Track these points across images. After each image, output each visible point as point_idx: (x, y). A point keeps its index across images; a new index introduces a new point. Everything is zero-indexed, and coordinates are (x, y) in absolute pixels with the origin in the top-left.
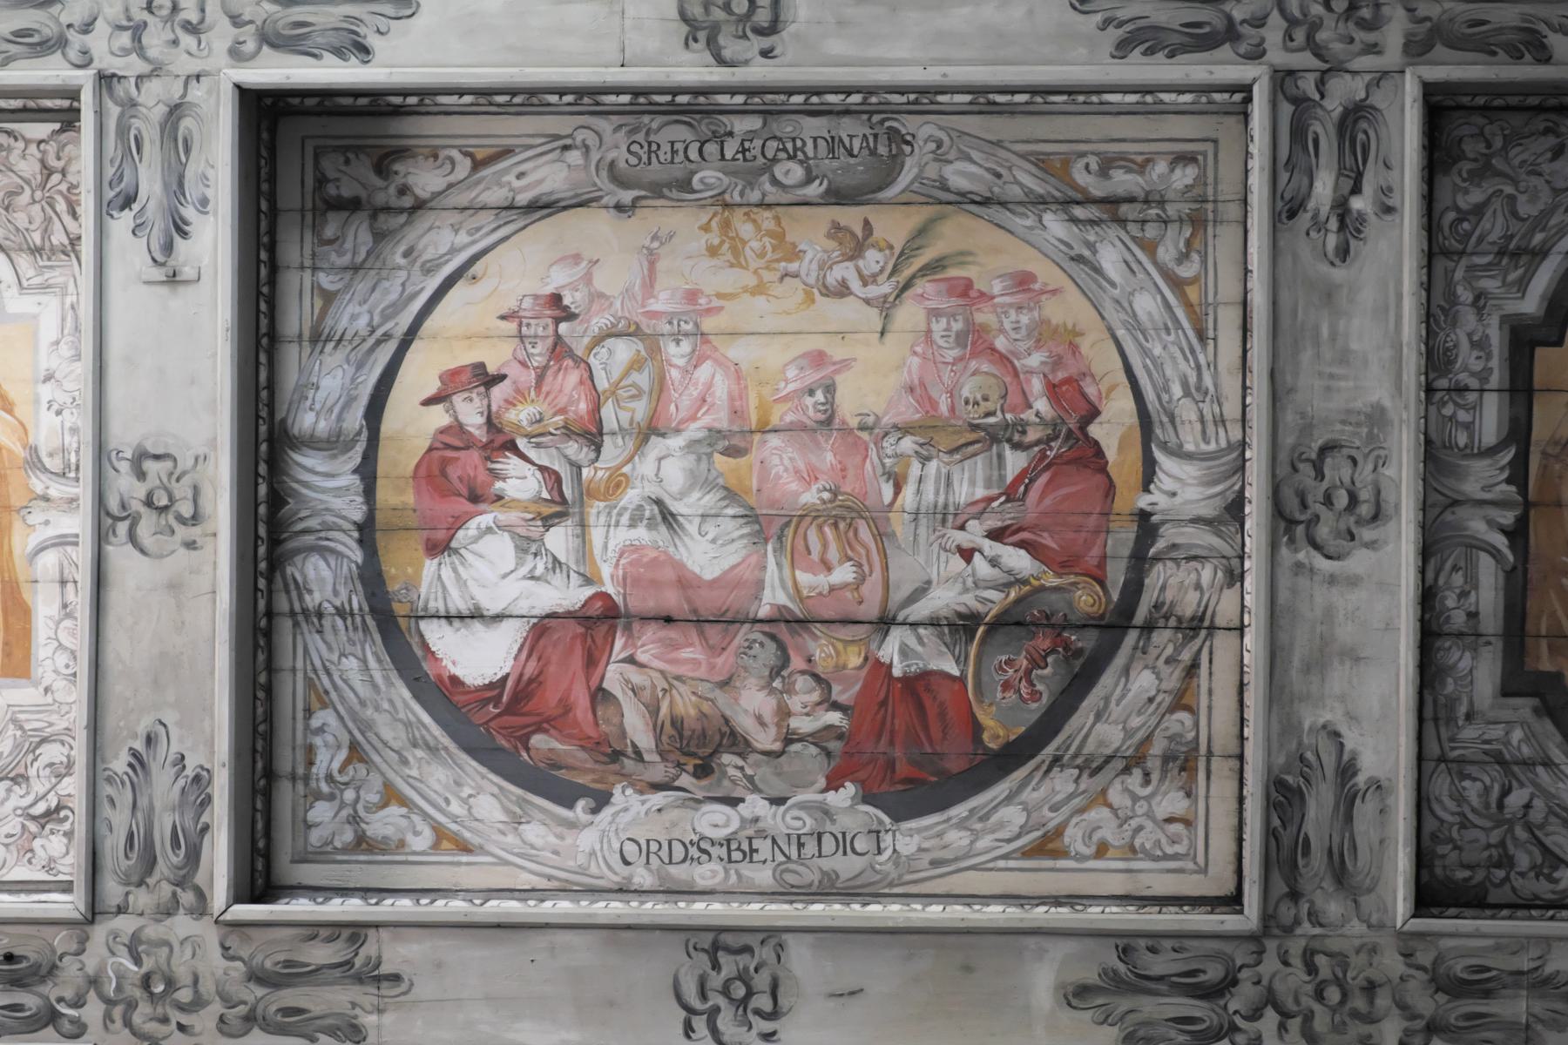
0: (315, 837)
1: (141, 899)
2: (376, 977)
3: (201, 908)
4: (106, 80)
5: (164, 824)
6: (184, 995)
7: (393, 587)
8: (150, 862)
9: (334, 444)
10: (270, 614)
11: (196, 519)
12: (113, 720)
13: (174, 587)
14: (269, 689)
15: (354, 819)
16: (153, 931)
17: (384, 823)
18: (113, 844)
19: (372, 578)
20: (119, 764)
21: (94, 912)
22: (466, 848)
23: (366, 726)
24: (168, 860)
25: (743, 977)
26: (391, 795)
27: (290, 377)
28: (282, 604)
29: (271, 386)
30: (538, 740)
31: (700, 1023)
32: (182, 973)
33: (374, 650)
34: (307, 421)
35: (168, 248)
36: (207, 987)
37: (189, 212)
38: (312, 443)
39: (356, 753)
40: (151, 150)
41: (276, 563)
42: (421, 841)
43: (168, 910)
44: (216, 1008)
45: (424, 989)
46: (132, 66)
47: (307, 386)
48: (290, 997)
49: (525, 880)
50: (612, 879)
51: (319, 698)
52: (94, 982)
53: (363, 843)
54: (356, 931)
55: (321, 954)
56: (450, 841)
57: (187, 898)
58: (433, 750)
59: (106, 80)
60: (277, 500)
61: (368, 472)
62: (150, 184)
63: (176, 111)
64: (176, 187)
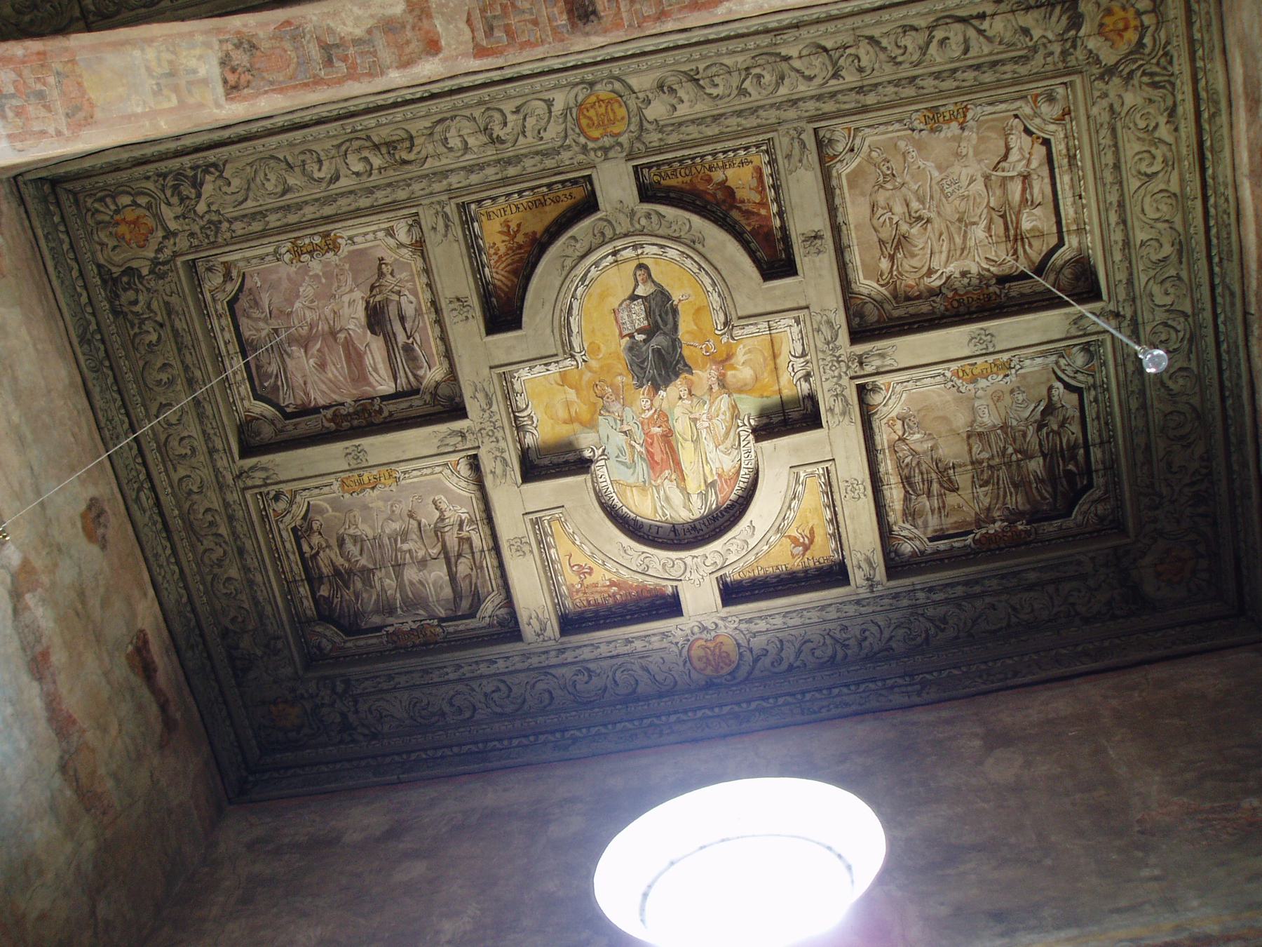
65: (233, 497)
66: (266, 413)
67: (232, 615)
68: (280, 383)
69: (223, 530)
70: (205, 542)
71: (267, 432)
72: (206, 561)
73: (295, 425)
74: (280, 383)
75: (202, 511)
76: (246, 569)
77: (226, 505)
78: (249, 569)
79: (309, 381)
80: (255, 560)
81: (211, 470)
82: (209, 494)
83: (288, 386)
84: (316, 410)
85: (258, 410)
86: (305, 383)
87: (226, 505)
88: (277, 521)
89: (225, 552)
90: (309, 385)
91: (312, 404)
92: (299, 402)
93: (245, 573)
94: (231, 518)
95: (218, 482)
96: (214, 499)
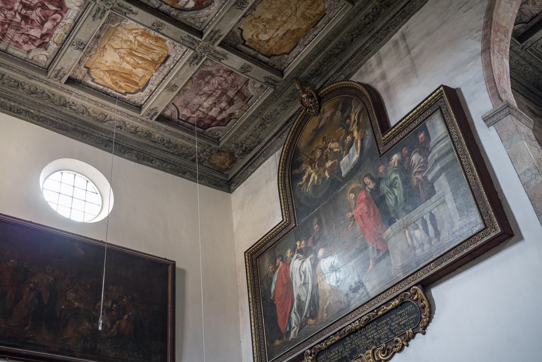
0: (199, 26)
1: (196, 46)
2: (217, 32)
3: (200, 42)
4: (111, 9)
5: (190, 40)
6: (207, 47)
7: (179, 8)
8: (193, 43)
9: (161, 5)
10: (174, 19)
11: (162, 24)
12: (177, 40)
13: (168, 29)
14: (182, 23)
15: (200, 22)
16: (200, 46)
17: (202, 20)
18: (189, 45)
19: (177, 9)
20: (182, 41)
21: (194, 50)
22: (209, 15)
23: (191, 17)
24: (194, 42)
25: (241, 3)
26: (199, 18)
27: (151, 5)
28: (174, 17)
29: (151, 7)
30: (203, 4)
31: (242, 8)
32: (205, 46)
33: (184, 12)
34: (157, 6)
35: (133, 12)
36: (208, 45)
37: (130, 9)
38: (159, 7)
39: (193, 19)
40: (121, 9)
41: (169, 16)
42: (206, 18)
43: (199, 44)
44: (210, 45)
45: (221, 28)
46: (111, 6)
47: (153, 4)
48: (214, 39)
49: (216, 11)
50: (221, 5)
51: (186, 19)
52: (201, 53)
53: (202, 23)
54: (212, 31)
55: (212, 35)
56: (207, 16)
57: (198, 42)
58: (198, 13)
59: (111, 9)
60: (163, 13)
61: (166, 4)
62: (125, 10)
63: (118, 4)
64: (126, 8)
65: (523, 53)
66: (520, 27)
67: (534, 78)
68: (522, 17)
69: (523, 62)
70: (518, 69)
71: (523, 31)
72: (520, 72)
73: (531, 23)
74: (522, 17)
75: (514, 63)
76: (534, 66)
77: (521, 57)
78: (535, 66)
79: (531, 10)
80: (536, 63)
81: (513, 52)
82: (514, 58)
83: (525, 16)
84: (537, 15)
85: (518, 27)
86: (530, 12)
87: (521, 57)
88: (535, 48)
89: (525, 67)
90: (532, 12)
91: (535, 15)
92: (530, 17)
93: (534, 68)
94: (524, 59)
95: (516, 53)
96: (517, 58)
